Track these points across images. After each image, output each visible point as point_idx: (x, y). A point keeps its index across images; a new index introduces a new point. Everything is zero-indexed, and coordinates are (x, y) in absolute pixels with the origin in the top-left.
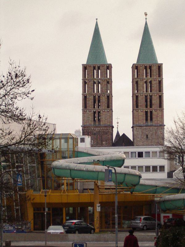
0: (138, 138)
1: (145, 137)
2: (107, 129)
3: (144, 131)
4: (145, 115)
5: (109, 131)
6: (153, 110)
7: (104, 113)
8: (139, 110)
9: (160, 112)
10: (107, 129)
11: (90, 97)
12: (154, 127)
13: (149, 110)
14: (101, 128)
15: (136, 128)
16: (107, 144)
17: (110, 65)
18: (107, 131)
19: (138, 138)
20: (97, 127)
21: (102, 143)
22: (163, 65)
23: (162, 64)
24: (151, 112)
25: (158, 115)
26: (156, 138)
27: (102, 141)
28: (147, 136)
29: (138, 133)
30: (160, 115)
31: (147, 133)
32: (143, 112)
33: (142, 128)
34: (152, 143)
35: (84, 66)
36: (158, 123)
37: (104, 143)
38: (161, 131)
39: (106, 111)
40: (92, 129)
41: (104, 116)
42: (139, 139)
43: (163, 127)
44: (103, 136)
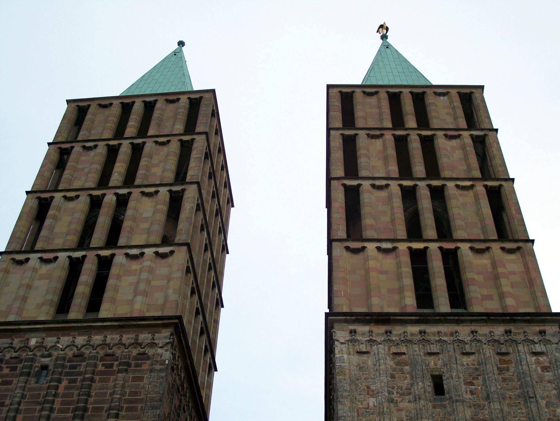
1: (425, 385)
2: (137, 344)
5: (150, 352)
6: (464, 247)
7: (135, 266)
8: (371, 247)
9: (512, 257)
10: (137, 344)
11: (71, 205)
12: (483, 330)
14: (97, 339)
15: (353, 332)
19: (370, 392)
24: (451, 259)
25: (500, 270)
29: (370, 361)
30: (513, 273)
31: (432, 361)
32: (397, 257)
33: (398, 330)
35: (74, 105)
38: (538, 348)
39: (149, 252)
40: (33, 342)
41: (132, 279)
42: (372, 401)
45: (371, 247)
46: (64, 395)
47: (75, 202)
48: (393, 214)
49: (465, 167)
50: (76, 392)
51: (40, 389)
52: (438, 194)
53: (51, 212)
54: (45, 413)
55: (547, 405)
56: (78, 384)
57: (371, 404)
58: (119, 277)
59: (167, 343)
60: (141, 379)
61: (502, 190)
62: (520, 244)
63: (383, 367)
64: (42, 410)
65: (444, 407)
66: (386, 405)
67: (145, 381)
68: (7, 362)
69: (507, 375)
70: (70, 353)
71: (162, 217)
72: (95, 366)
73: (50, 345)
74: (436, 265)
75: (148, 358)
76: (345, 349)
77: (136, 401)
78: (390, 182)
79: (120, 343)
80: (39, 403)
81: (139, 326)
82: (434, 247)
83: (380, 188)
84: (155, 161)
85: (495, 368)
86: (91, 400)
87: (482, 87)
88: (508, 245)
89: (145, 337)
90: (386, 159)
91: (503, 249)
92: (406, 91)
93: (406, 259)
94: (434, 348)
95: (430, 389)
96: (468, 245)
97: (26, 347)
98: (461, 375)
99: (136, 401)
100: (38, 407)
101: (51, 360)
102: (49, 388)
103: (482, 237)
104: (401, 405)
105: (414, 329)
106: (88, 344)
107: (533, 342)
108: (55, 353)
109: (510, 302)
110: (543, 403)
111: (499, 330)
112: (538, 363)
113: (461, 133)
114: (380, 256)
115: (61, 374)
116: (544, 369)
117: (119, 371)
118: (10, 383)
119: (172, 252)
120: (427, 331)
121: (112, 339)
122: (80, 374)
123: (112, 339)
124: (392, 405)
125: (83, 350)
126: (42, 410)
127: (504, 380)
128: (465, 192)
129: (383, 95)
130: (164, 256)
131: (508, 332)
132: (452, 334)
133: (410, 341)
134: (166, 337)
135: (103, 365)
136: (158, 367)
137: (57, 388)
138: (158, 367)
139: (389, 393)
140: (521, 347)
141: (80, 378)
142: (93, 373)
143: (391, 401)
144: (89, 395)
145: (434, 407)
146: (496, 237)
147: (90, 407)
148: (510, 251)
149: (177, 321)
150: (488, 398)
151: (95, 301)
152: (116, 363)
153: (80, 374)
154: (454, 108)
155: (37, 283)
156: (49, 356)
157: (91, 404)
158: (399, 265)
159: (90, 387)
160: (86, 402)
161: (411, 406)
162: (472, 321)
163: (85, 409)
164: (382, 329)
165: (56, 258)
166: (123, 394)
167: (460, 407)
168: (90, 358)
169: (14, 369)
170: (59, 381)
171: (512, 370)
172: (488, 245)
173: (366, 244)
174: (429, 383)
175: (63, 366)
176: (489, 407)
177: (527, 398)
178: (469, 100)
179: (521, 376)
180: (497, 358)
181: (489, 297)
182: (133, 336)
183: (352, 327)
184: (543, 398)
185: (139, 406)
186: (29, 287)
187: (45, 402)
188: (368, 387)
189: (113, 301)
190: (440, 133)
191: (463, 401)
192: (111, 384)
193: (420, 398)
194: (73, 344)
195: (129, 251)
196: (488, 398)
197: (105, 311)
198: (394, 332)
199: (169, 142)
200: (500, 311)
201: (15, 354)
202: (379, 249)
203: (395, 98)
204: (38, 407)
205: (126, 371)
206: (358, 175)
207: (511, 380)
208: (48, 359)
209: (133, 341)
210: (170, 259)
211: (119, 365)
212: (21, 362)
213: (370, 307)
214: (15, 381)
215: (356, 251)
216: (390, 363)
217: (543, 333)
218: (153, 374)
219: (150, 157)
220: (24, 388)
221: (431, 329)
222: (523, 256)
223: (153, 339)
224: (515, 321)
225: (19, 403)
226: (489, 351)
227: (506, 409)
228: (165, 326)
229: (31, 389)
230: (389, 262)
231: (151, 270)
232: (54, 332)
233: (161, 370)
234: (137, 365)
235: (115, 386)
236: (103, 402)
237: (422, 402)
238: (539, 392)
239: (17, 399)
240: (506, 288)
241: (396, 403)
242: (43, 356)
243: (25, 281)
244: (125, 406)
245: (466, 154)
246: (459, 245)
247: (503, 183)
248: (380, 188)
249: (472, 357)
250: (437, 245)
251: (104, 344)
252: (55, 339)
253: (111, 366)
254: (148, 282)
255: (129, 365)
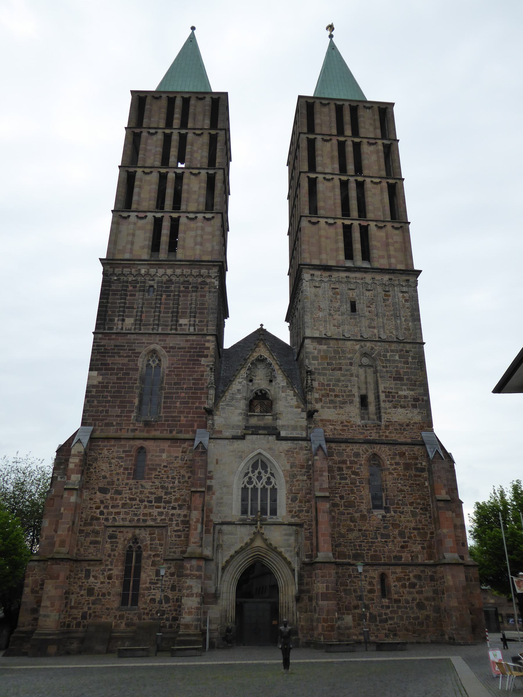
0: (320, 309)
1: (347, 307)
2: (201, 276)
3: (343, 288)
4: (341, 238)
5: (208, 280)
6: (372, 224)
7: (192, 224)
8: (322, 221)
9: (397, 232)
10: (201, 276)
11: (148, 177)
12: (378, 277)
13: (356, 223)
14: (178, 271)
15: (312, 275)
16: (194, 325)
17: (223, 97)
18: (200, 280)
20: (160, 264)
21: (177, 321)
22: (395, 108)
23: (393, 104)
24: (364, 231)
25: (390, 241)
26: (387, 313)
27: (176, 315)
28: (353, 308)
29: (320, 291)
30: (396, 242)
31: (351, 293)
32: (336, 228)
33: (335, 275)
34: (376, 331)
35: (136, 95)
36: (390, 264)
37: (182, 321)
38: (405, 289)
39: (200, 216)
40: (143, 271)
41: (192, 233)
42: (321, 314)
43: (412, 279)
44: (181, 299)
45: (322, 221)
46: (165, 304)
47: (150, 176)
48: (335, 199)
49: (377, 167)
50: (171, 302)
51: (152, 299)
52: (360, 185)
53: (137, 183)
54: (157, 314)
55: (405, 320)
56: (172, 297)
57: (320, 316)
58: (185, 233)
59: (217, 276)
60: (204, 296)
61: (397, 185)
62: (402, 224)
63: (327, 296)
64: (155, 312)
65: (355, 319)
66: (328, 316)
67: (207, 297)
68: (130, 283)
69: (388, 303)
70: (165, 279)
71: (204, 192)
72: (179, 287)
73: (153, 274)
74: (356, 235)
75: (207, 284)
76: (308, 285)
77: (203, 309)
78: (334, 176)
79: (191, 275)
80: (152, 308)
81: (200, 265)
82: (356, 223)
83: (328, 180)
84: (195, 148)
85: (382, 299)
86: (180, 307)
87: (393, 104)
88: (397, 225)
89: (204, 271)
90: (332, 158)
91: (393, 227)
92: (347, 104)
93: (341, 231)
94: (353, 286)
95: (349, 309)
96: (375, 223)
97: (140, 274)
98: (365, 302)
99: (203, 309)
100: (153, 310)
101: (155, 283)
102: (156, 299)
103: (382, 219)
104: (335, 317)
105: (343, 275)
106: (174, 274)
107: (402, 286)
108: (156, 279)
109: (393, 261)
110: (403, 319)
111: (386, 277)
112: (403, 297)
113: (377, 141)
114: (327, 227)
115: (161, 291)
116: (406, 301)
117: (193, 291)
118: (135, 295)
119: (213, 217)
120: (350, 276)
121: (186, 272)
122: (171, 291)
123: (186, 272)
124: (331, 317)
125: (171, 278)
126: (155, 312)
127: (386, 306)
128: (375, 186)
129: (333, 107)
130: (208, 219)
131: (390, 279)
132: (362, 279)
133: (341, 282)
134: (215, 272)
135: (183, 287)
136: (213, 290)
137: (161, 299)
138: (213, 290)
139: (330, 310)
140: (396, 288)
141: (172, 294)
142: (179, 292)
143: (330, 314)
144: (178, 304)
145: (351, 319)
146: (389, 219)
147: (180, 311)
148: (397, 229)
149: (221, 264)
150: (377, 315)
151: (173, 246)
152: (190, 286)
153: (171, 291)
154: (374, 120)
155: (138, 233)
156: (153, 280)
157: (181, 309)
158: (337, 234)
159: (178, 300)
160: (178, 308)
161: (340, 317)
162: (373, 272)
163: (178, 312)
164: (327, 274)
165: (146, 216)
166: (196, 305)
167: (363, 319)
168: (176, 283)
169: (135, 287)
170: (161, 295)
171: (390, 300)
172: (385, 224)
173: (320, 219)
174: (349, 305)
175: (162, 287)
176: (377, 320)
177: (396, 317)
178: (384, 112)
179: (394, 304)
180: (383, 293)
181: (382, 257)
182: (198, 270)
183: (312, 272)
184: (403, 317)
185: (206, 311)
186: (134, 235)
187: (156, 307)
188: (319, 306)
189: (184, 248)
190: (365, 141)
191: (365, 317)
192: (189, 298)
193: (344, 314)
194: (165, 274)
195: (188, 215)
196: (377, 315)
197: (180, 254)
198: (333, 276)
199: (202, 133)
200: (388, 268)
201: (134, 279)
202: (326, 222)
203: (339, 109)
204: (153, 310)
205: (196, 291)
206: (315, 170)
207: (389, 306)
208: (153, 282)
209: (198, 274)
210: (212, 221)
211: (192, 287)
212: (138, 283)
213: (321, 260)
214: (137, 294)
215: (314, 223)
216: (331, 293)
217: (408, 281)
218: (211, 294)
219: (192, 145)
220: (143, 299)
221: (352, 275)
222: (403, 232)
223: (209, 273)
224: (394, 273)
225: (142, 308)
226: (380, 289)
227: (385, 322)
228: (214, 266)
229: (147, 300)
230: (331, 231)
231: (203, 229)
232: (154, 266)
233: (215, 292)
234: (202, 288)
235: (191, 300)
236: (186, 308)
237: (345, 316)
238: (402, 313)
239: (140, 305)
240: (392, 253)
241: (333, 316)
242: (150, 280)
243: (131, 231)
244: (198, 311)
245: (378, 157)
246: (370, 223)
247: (398, 181)
248: (328, 180)
249: (371, 292)
250: (358, 222)
251: (182, 275)
252: (155, 270)
253: (188, 288)
254: (202, 236)
255: (197, 288)
